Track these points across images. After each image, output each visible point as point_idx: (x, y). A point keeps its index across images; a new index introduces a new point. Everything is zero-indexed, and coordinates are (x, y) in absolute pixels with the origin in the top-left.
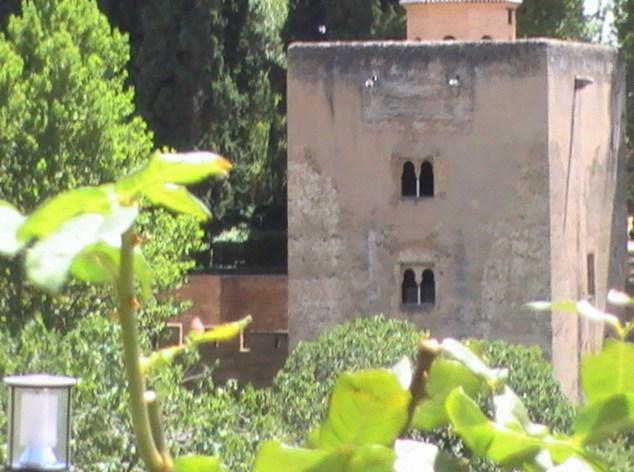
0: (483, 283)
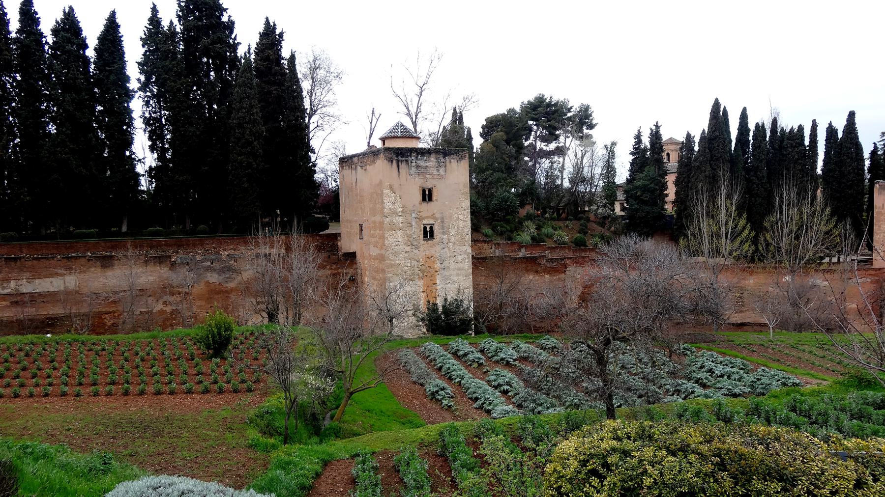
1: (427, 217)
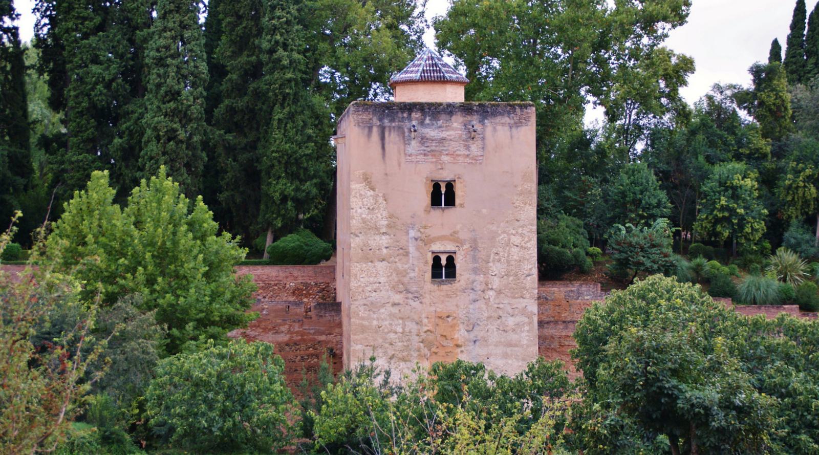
0: (491, 264)
1: (441, 238)
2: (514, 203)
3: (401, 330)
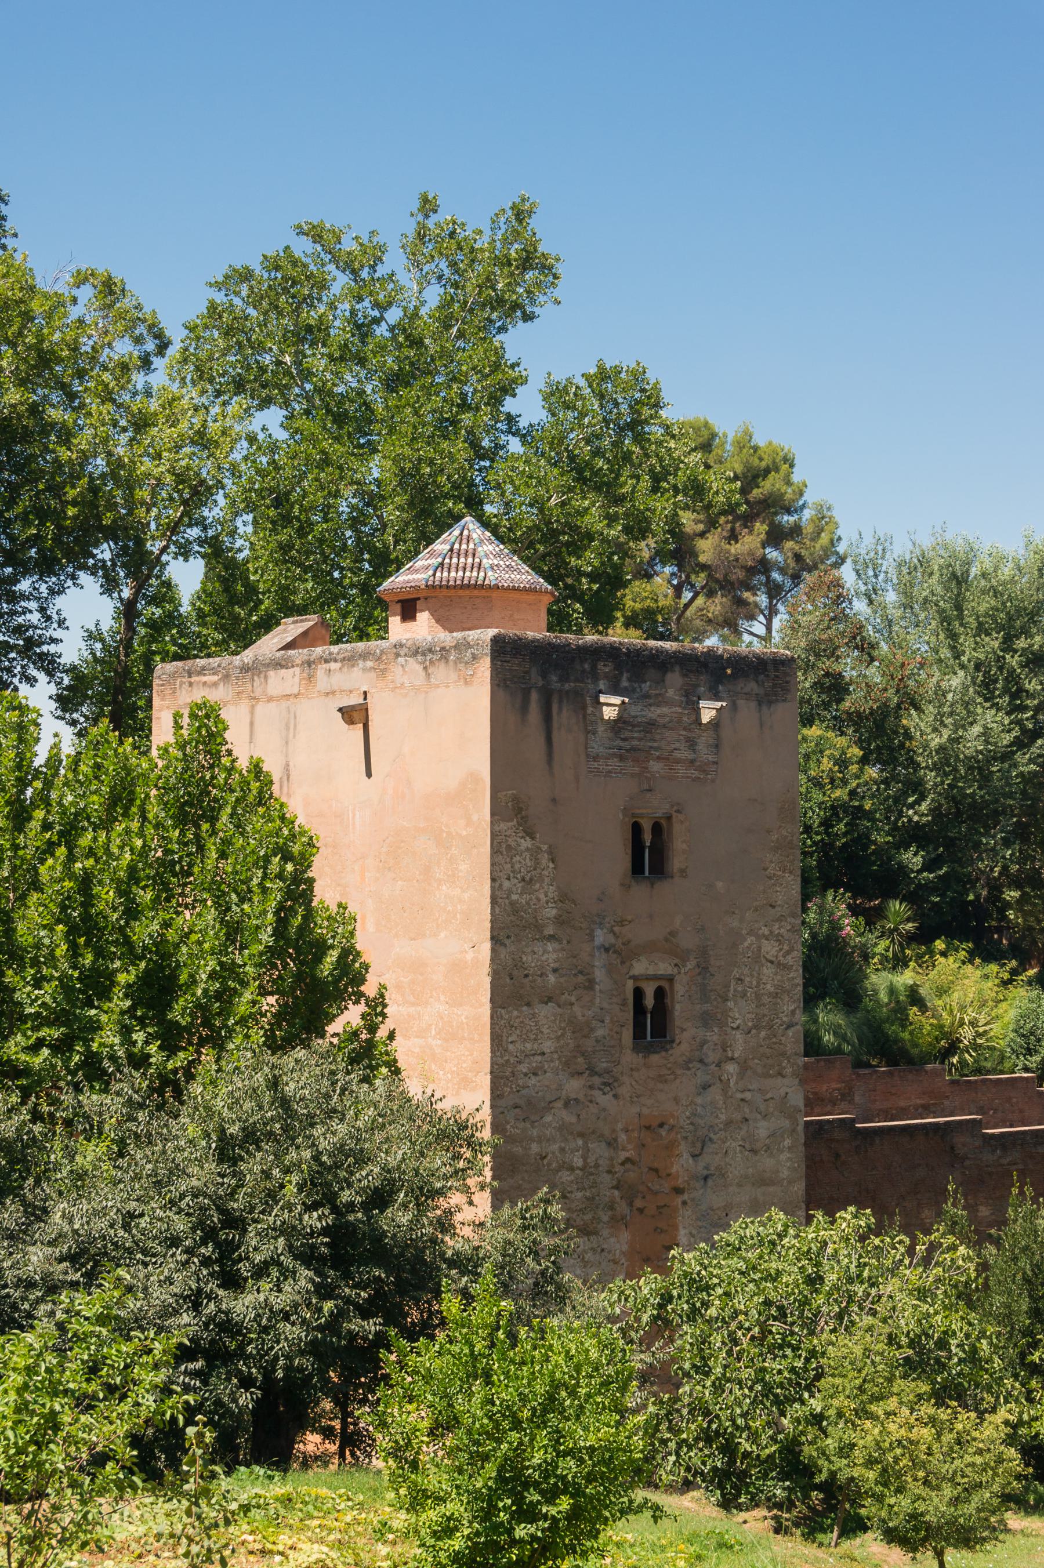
2: (765, 869)
3: (579, 1162)
